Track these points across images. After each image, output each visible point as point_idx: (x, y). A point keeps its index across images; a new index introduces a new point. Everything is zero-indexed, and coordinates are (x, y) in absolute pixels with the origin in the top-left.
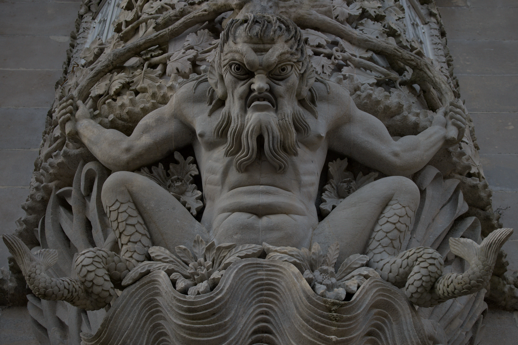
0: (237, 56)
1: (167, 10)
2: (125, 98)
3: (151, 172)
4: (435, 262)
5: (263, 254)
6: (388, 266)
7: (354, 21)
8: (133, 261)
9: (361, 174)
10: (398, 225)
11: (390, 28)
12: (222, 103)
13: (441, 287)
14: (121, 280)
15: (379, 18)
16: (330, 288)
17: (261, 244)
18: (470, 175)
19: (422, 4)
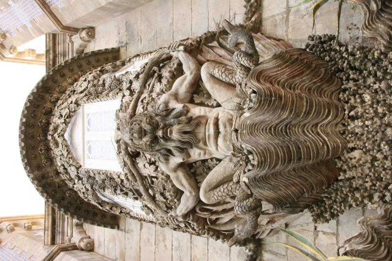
0: (148, 143)
1: (128, 177)
2: (167, 194)
3: (200, 182)
4: (239, 54)
7: (132, 93)
8: (240, 189)
9: (200, 89)
10: (223, 71)
11: (135, 78)
12: (169, 151)
13: (250, 52)
14: (248, 195)
15: (131, 82)
16: (251, 101)
17: (232, 132)
18: (201, 41)
19: (125, 65)
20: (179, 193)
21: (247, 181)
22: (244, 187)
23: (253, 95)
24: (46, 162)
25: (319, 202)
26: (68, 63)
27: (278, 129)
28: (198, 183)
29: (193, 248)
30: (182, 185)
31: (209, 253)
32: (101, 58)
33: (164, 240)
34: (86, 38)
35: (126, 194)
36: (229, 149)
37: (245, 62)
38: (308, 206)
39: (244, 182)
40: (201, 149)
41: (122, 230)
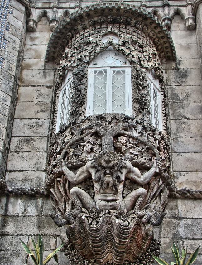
5: (109, 213)
6: (139, 214)
8: (79, 212)
16: (124, 221)
17: (108, 210)
20: (74, 168)
21: (83, 217)
22: (79, 216)
23: (128, 224)
24: (91, 23)
25: (73, 248)
26: (164, 32)
27: (109, 235)
28: (81, 184)
29: (39, 139)
30: (80, 176)
31: (37, 153)
32: (169, 50)
33: (42, 111)
34: (187, 24)
35: (72, 114)
36: (99, 206)
37: (145, 219)
38: (70, 242)
39: (82, 216)
40: (100, 190)
41: (45, 66)
